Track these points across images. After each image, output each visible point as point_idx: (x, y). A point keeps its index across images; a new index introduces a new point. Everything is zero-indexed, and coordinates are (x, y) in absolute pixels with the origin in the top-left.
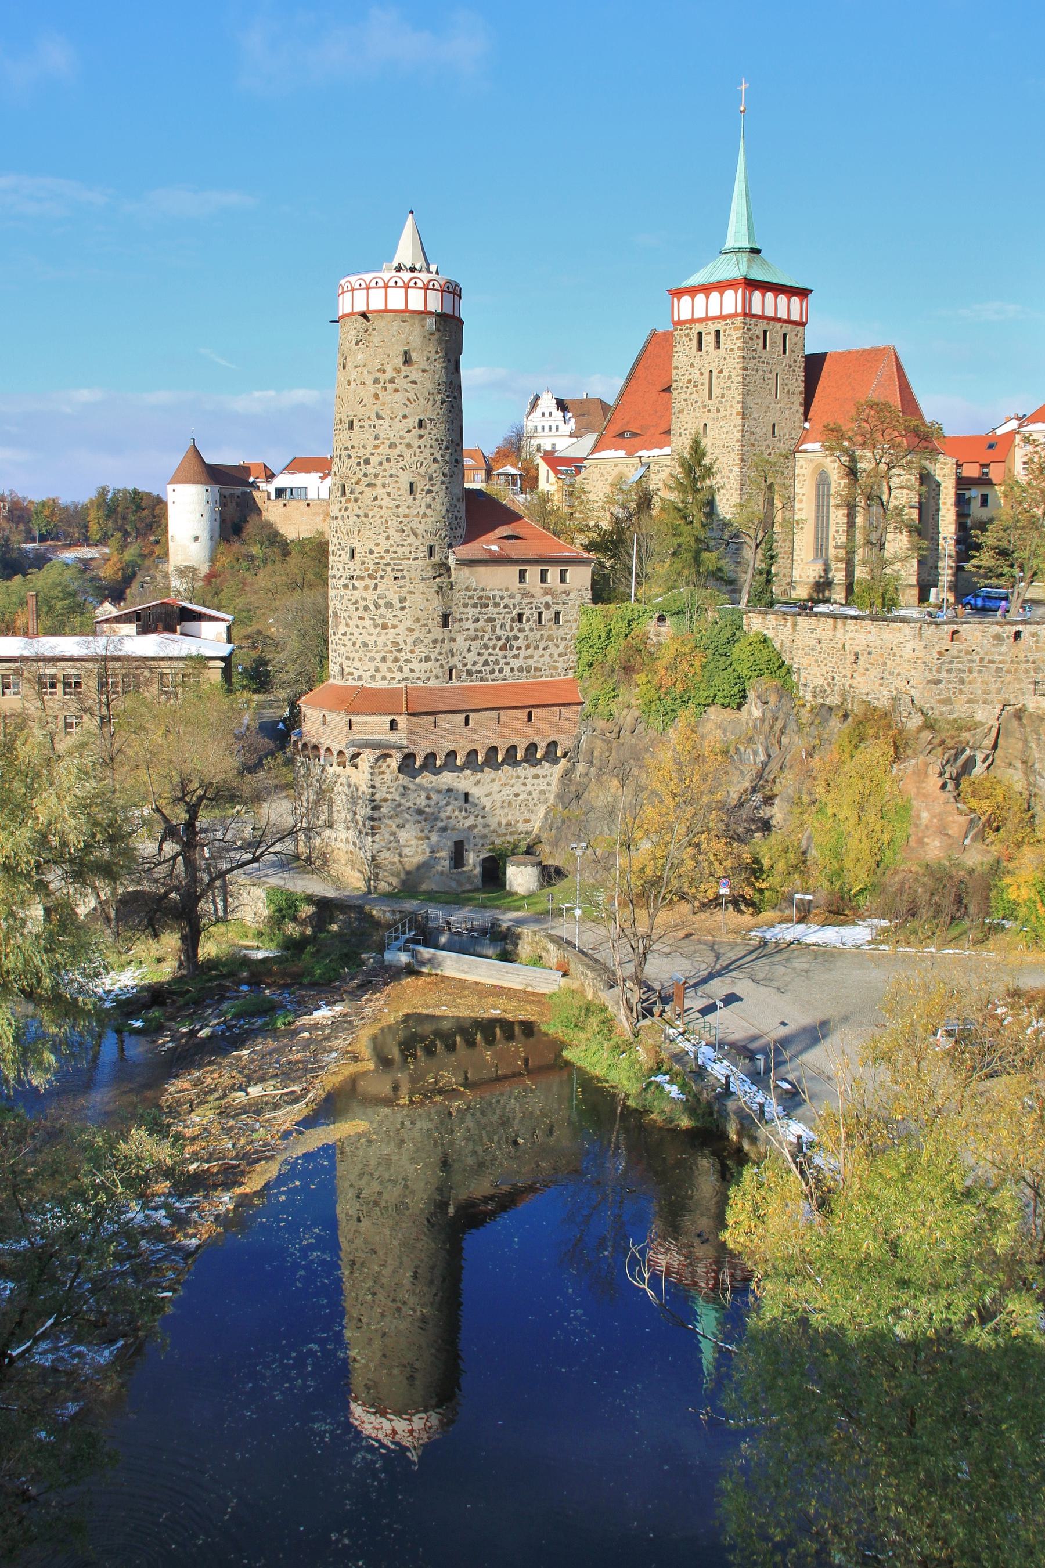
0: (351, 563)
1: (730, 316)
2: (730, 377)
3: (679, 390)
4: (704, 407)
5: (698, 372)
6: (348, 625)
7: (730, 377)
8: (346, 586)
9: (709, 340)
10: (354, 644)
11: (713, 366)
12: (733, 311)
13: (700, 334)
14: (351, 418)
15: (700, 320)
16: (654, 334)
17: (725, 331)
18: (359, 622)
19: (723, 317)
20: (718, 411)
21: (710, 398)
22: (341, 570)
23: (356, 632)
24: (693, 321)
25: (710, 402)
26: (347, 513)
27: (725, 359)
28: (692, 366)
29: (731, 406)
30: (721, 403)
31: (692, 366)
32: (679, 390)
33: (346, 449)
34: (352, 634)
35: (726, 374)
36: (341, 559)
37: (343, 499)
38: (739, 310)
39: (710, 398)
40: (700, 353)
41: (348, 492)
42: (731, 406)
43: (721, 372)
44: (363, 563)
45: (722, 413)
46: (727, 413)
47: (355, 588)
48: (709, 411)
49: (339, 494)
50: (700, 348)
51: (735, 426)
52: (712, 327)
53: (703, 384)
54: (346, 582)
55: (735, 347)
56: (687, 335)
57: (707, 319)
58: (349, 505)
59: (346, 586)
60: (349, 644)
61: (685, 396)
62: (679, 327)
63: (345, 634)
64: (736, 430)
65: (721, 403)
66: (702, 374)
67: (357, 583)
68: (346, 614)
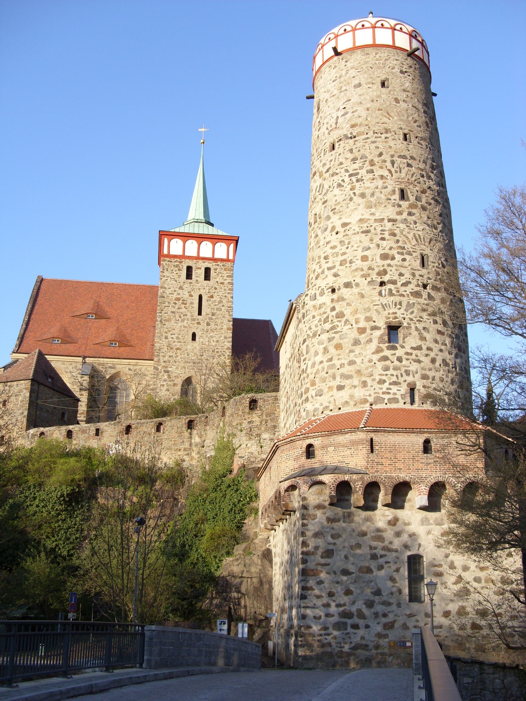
0: (424, 271)
1: (222, 260)
2: (220, 302)
3: (167, 304)
4: (194, 320)
5: (187, 295)
6: (423, 338)
7: (220, 302)
8: (417, 294)
9: (199, 274)
10: (433, 361)
11: (202, 292)
12: (224, 257)
13: (189, 269)
14: (406, 131)
15: (189, 258)
16: (41, 281)
17: (216, 269)
18: (439, 337)
19: (214, 259)
20: (208, 324)
21: (200, 313)
22: (407, 276)
23: (436, 347)
24: (183, 257)
25: (200, 317)
26: (413, 218)
27: (216, 289)
28: (181, 288)
29: (222, 323)
30: (211, 319)
31: (181, 288)
32: (167, 304)
33: (404, 157)
34: (429, 349)
35: (216, 298)
36: (406, 264)
37: (405, 204)
38: (231, 257)
39: (200, 313)
40: (190, 281)
41: (412, 199)
42: (222, 323)
43: (212, 297)
44: (438, 274)
45: (212, 325)
46: (219, 327)
47: (430, 297)
48: (199, 323)
49: (397, 196)
50: (189, 276)
51: (225, 338)
52: (204, 265)
53: (192, 303)
54: (418, 289)
55: (226, 282)
56: (177, 266)
57: (198, 258)
58: (414, 211)
59: (417, 294)
60: (426, 361)
61: (173, 310)
62: (168, 259)
63: (419, 348)
64: (226, 340)
65: (211, 319)
66: (191, 296)
67: (433, 293)
68: (420, 326)
